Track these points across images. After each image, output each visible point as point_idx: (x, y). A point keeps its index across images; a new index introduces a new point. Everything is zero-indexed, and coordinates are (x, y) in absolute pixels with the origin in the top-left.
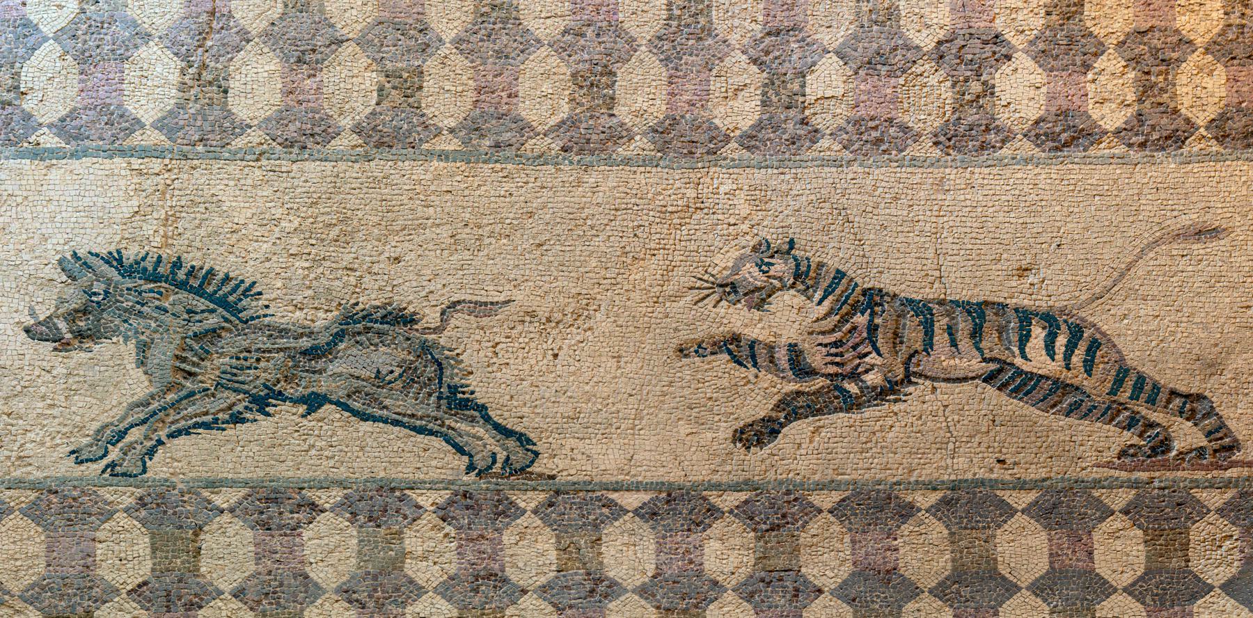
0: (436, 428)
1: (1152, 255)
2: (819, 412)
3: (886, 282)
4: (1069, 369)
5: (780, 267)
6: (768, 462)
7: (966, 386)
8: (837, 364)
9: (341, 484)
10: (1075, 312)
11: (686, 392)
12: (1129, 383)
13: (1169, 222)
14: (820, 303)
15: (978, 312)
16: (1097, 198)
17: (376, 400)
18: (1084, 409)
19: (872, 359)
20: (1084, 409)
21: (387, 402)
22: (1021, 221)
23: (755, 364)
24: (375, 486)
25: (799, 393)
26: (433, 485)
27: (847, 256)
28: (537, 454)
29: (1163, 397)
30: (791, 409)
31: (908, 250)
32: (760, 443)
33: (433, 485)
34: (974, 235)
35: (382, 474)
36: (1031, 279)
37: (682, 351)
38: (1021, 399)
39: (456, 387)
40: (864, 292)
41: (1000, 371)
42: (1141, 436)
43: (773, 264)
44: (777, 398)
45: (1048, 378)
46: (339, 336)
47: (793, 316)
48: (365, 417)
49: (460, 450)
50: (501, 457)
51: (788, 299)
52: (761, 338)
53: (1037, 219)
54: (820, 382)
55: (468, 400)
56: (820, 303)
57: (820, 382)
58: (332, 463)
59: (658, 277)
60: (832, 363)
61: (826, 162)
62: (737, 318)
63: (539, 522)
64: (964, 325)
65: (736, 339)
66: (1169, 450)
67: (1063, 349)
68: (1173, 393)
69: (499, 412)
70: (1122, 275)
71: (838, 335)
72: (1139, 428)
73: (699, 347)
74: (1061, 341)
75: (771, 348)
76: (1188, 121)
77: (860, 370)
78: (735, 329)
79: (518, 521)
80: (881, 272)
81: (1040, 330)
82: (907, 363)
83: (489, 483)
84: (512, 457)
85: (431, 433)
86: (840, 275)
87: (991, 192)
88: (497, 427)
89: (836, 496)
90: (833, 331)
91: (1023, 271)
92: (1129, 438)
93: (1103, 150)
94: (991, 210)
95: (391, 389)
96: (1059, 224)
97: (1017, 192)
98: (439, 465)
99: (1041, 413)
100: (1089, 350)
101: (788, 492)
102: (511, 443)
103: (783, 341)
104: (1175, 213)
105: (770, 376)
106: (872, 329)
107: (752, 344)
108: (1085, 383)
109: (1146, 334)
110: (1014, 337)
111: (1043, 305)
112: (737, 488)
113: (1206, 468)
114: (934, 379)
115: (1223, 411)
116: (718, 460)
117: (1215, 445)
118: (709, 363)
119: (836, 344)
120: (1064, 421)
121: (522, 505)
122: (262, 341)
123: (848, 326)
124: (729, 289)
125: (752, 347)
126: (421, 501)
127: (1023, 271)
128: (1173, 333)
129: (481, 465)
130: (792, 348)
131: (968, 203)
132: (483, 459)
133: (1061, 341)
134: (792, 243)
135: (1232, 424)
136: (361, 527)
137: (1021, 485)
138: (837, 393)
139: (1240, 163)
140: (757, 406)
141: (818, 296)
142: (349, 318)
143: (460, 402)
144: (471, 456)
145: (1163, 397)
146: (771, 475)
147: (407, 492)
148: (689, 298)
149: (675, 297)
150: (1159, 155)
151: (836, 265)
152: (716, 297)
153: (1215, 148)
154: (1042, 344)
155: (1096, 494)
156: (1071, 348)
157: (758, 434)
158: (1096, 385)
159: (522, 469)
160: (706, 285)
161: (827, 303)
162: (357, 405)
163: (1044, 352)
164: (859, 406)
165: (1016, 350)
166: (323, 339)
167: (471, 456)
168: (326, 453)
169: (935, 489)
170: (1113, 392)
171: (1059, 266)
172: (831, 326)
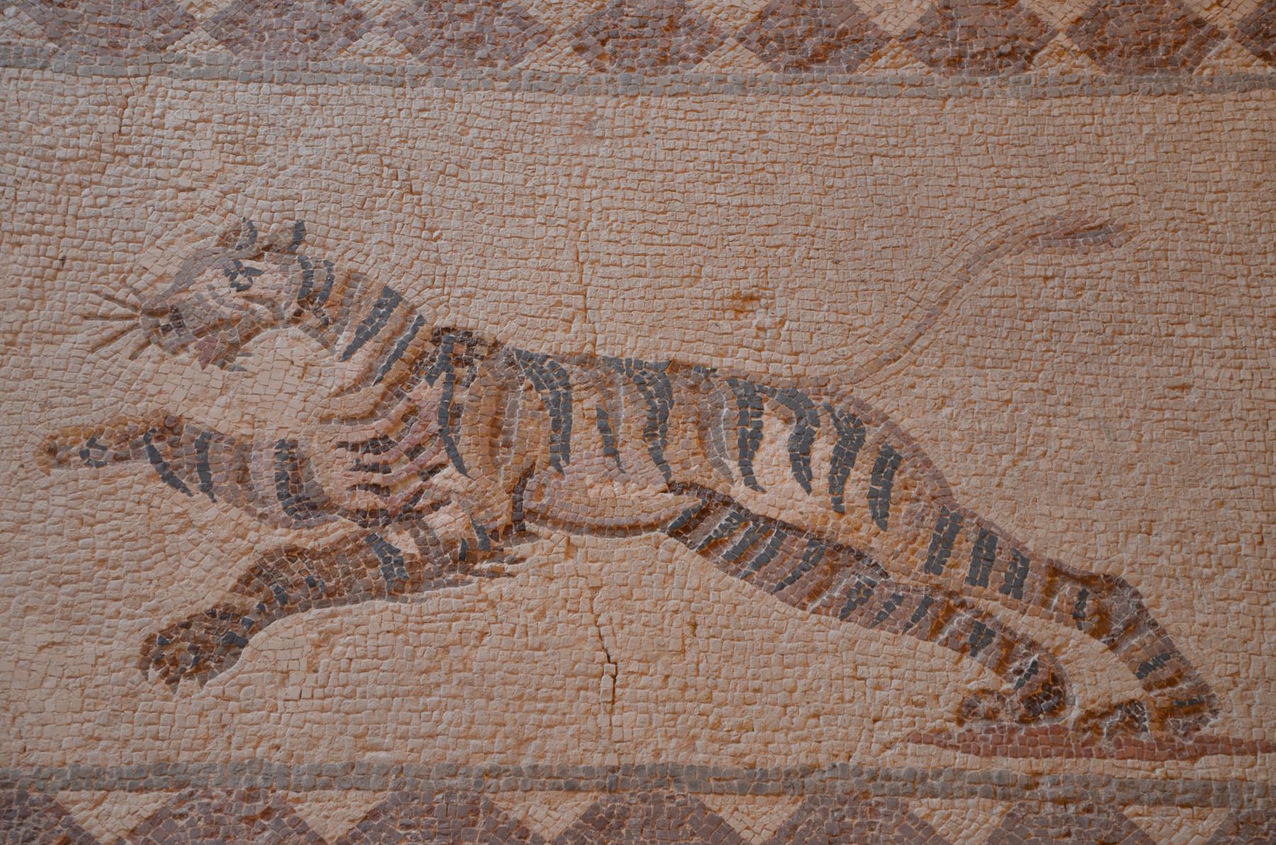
1: (986, 275)
2: (331, 597)
3: (476, 317)
4: (842, 513)
5: (273, 278)
6: (212, 716)
7: (638, 544)
8: (377, 488)
10: (845, 388)
11: (51, 546)
12: (965, 545)
13: (1013, 211)
14: (347, 355)
15: (660, 383)
16: (877, 160)
18: (877, 603)
19: (446, 479)
20: (877, 603)
22: (736, 201)
23: (207, 488)
25: (293, 552)
27: (405, 261)
29: (1035, 580)
30: (275, 587)
31: (523, 253)
32: (200, 669)
34: (648, 226)
36: (760, 317)
38: (747, 577)
40: (438, 336)
41: (703, 512)
42: (1000, 667)
43: (259, 273)
44: (246, 562)
45: (799, 531)
47: (292, 382)
51: (283, 346)
52: (223, 428)
53: (767, 199)
54: (338, 528)
56: (347, 355)
57: (338, 528)
59: (21, 289)
60: (368, 487)
61: (372, 76)
62: (179, 385)
64: (630, 414)
65: (169, 427)
66: (1061, 703)
67: (827, 467)
68: (1056, 571)
70: (932, 316)
71: (378, 426)
72: (993, 651)
73: (92, 443)
74: (822, 449)
75: (242, 449)
76: (1034, 19)
77: (422, 502)
78: (170, 408)
80: (470, 296)
81: (779, 425)
82: (517, 488)
86: (390, 298)
87: (680, 144)
89: (357, 804)
90: (371, 415)
91: (744, 302)
92: (974, 673)
93: (882, 70)
94: (680, 178)
96: (807, 209)
97: (728, 146)
99: (791, 611)
100: (878, 470)
101: (251, 795)
103: (269, 434)
104: (1024, 194)
105: (235, 512)
106: (450, 414)
107: (204, 442)
108: (875, 543)
110: (730, 440)
111: (783, 370)
112: (137, 782)
113: (1141, 752)
114: (574, 527)
115: (1162, 613)
116: (104, 711)
117: (1160, 697)
118: (108, 480)
119: (374, 445)
120: (840, 630)
124: (166, 320)
125: (202, 447)
127: (744, 302)
128: (1042, 438)
130: (289, 454)
131: (638, 163)
133: (822, 449)
134: (299, 232)
135: (1186, 646)
137: (755, 783)
138: (373, 555)
139: (1136, 98)
140: (202, 578)
141: (343, 341)
145: (1035, 580)
146: (216, 751)
148: (80, 338)
149: (57, 333)
151: (383, 278)
152: (138, 336)
153: (1087, 69)
154: (784, 454)
155: (919, 808)
156: (842, 462)
157: (196, 648)
158: (896, 547)
160: (120, 310)
161: (360, 356)
163: (789, 473)
164: (417, 585)
165: (733, 465)
169: (572, 788)
170: (933, 566)
171: (810, 293)
172: (366, 406)
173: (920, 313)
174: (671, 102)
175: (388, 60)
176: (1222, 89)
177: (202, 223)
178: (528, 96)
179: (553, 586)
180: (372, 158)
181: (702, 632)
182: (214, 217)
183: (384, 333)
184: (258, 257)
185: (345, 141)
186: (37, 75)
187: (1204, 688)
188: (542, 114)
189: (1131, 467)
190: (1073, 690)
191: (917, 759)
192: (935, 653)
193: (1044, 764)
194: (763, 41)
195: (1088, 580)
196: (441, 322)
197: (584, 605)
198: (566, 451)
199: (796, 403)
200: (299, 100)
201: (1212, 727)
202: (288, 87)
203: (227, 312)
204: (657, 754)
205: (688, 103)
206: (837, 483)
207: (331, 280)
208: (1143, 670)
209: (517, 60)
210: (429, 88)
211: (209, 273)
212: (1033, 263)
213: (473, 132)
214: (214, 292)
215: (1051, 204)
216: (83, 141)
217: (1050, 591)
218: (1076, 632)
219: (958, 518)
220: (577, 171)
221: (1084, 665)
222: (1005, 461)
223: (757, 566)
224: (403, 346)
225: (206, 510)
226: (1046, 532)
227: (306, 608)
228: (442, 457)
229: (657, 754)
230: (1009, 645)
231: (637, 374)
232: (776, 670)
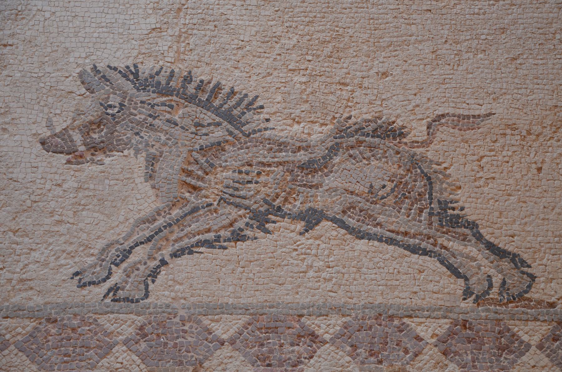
0: (429, 247)
9: (339, 310)
17: (370, 216)
21: (381, 218)
24: (373, 314)
26: (431, 313)
28: (533, 277)
33: (431, 313)
35: (379, 300)
39: (446, 203)
46: (334, 150)
48: (360, 235)
49: (455, 272)
50: (497, 280)
55: (458, 217)
58: (329, 286)
63: (546, 360)
69: (490, 230)
79: (524, 358)
83: (488, 310)
84: (509, 281)
85: (425, 252)
88: (490, 246)
95: (384, 205)
98: (436, 289)
102: (505, 264)
121: (525, 338)
122: (262, 154)
126: (420, 331)
129: (478, 289)
132: (479, 282)
136: (363, 363)
142: (342, 132)
143: (452, 220)
144: (466, 279)
147: (405, 320)
159: (521, 296)
162: (351, 222)
166: (320, 152)
167: (466, 279)
168: (324, 275)
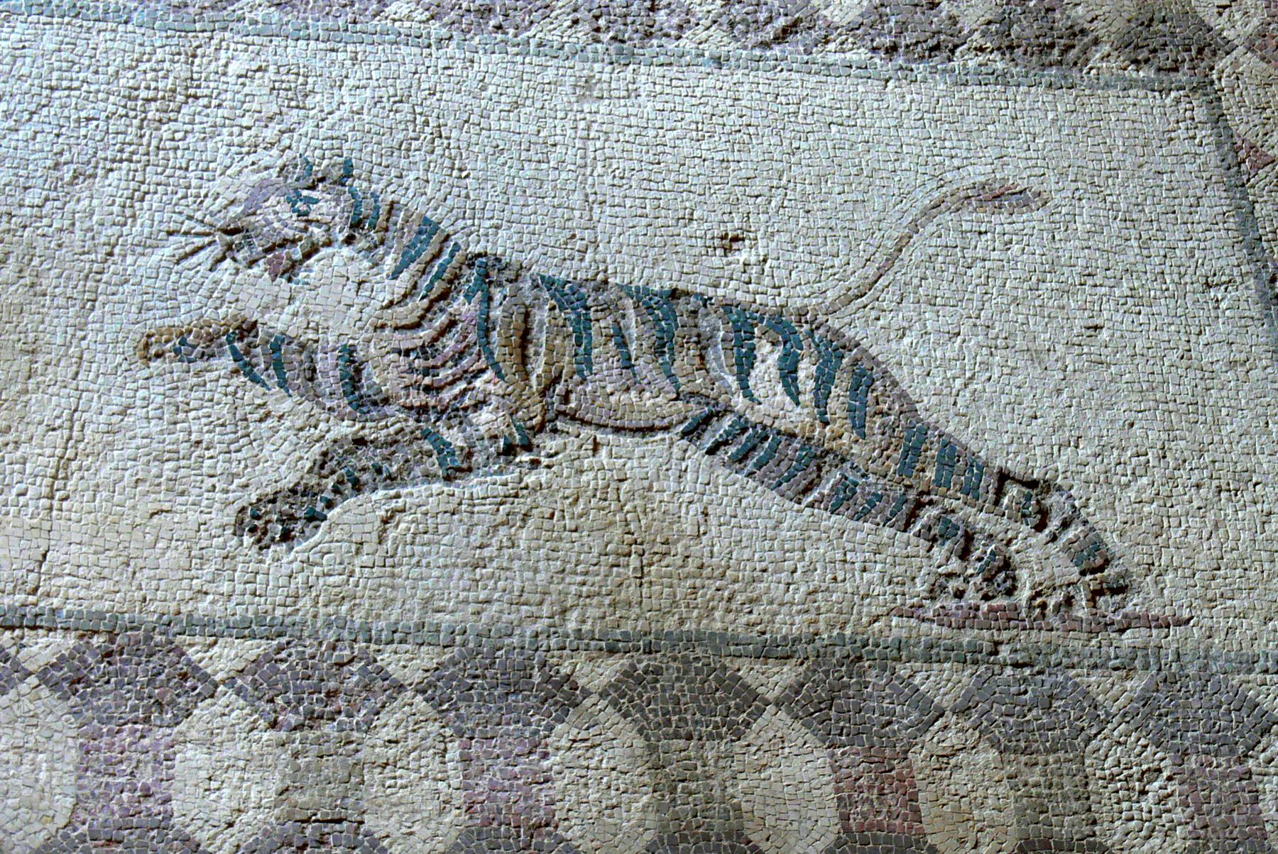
1: (931, 228)
3: (502, 244)
4: (826, 423)
5: (325, 205)
8: (428, 389)
10: (821, 318)
13: (949, 176)
14: (395, 275)
16: (834, 128)
22: (719, 156)
23: (283, 384)
27: (440, 195)
31: (541, 192)
34: (646, 174)
36: (743, 256)
37: (148, 351)
38: (750, 474)
41: (707, 420)
45: (793, 436)
47: (349, 293)
52: (292, 332)
53: (744, 156)
56: (395, 275)
59: (116, 209)
62: (249, 290)
65: (246, 329)
67: (811, 384)
68: (1004, 477)
73: (183, 343)
78: (245, 313)
80: (498, 227)
81: (768, 347)
86: (428, 227)
87: (668, 106)
90: (417, 326)
91: (730, 242)
94: (670, 135)
96: (780, 166)
97: (709, 109)
99: (788, 504)
100: (854, 389)
104: (956, 162)
105: (307, 405)
109: (945, 363)
111: (771, 302)
118: (197, 374)
123: (441, 320)
125: (276, 349)
128: (987, 366)
131: (633, 121)
133: (806, 370)
138: (427, 446)
139: (1041, 90)
141: (389, 262)
148: (167, 251)
149: (147, 245)
150: (920, 69)
151: (421, 209)
154: (775, 373)
156: (824, 382)
160: (199, 229)
161: (405, 275)
165: (732, 381)
170: (906, 468)
171: (784, 237)
172: (412, 319)
173: (880, 258)
174: (659, 71)
175: (415, 25)
176: (1107, 85)
177: (265, 158)
178: (536, 60)
179: (584, 478)
180: (406, 107)
181: (713, 520)
182: (275, 152)
183: (425, 256)
184: (313, 187)
185: (383, 92)
186: (121, 28)
187: (1125, 574)
188: (550, 74)
189: (1059, 392)
190: (1023, 574)
191: (898, 628)
192: (907, 542)
193: (1005, 635)
194: (732, 25)
195: (1032, 484)
196: (474, 249)
197: (611, 495)
198: (590, 364)
199: (782, 327)
200: (341, 56)
201: (1134, 604)
202: (329, 45)
203: (289, 233)
204: (682, 622)
205: (673, 72)
206: (821, 399)
207: (377, 208)
208: (1076, 559)
209: (527, 29)
210: (452, 49)
211: (273, 200)
212: (969, 219)
213: (491, 89)
214: (277, 216)
215: (977, 173)
216: (161, 85)
217: (1000, 493)
218: (1023, 527)
219: (924, 432)
220: (582, 125)
221: (1033, 554)
222: (958, 383)
223: (759, 465)
224: (443, 268)
225: (282, 403)
226: (995, 443)
227: (374, 490)
228: (482, 364)
229: (682, 622)
230: (969, 538)
231: (645, 300)
232: (778, 554)
